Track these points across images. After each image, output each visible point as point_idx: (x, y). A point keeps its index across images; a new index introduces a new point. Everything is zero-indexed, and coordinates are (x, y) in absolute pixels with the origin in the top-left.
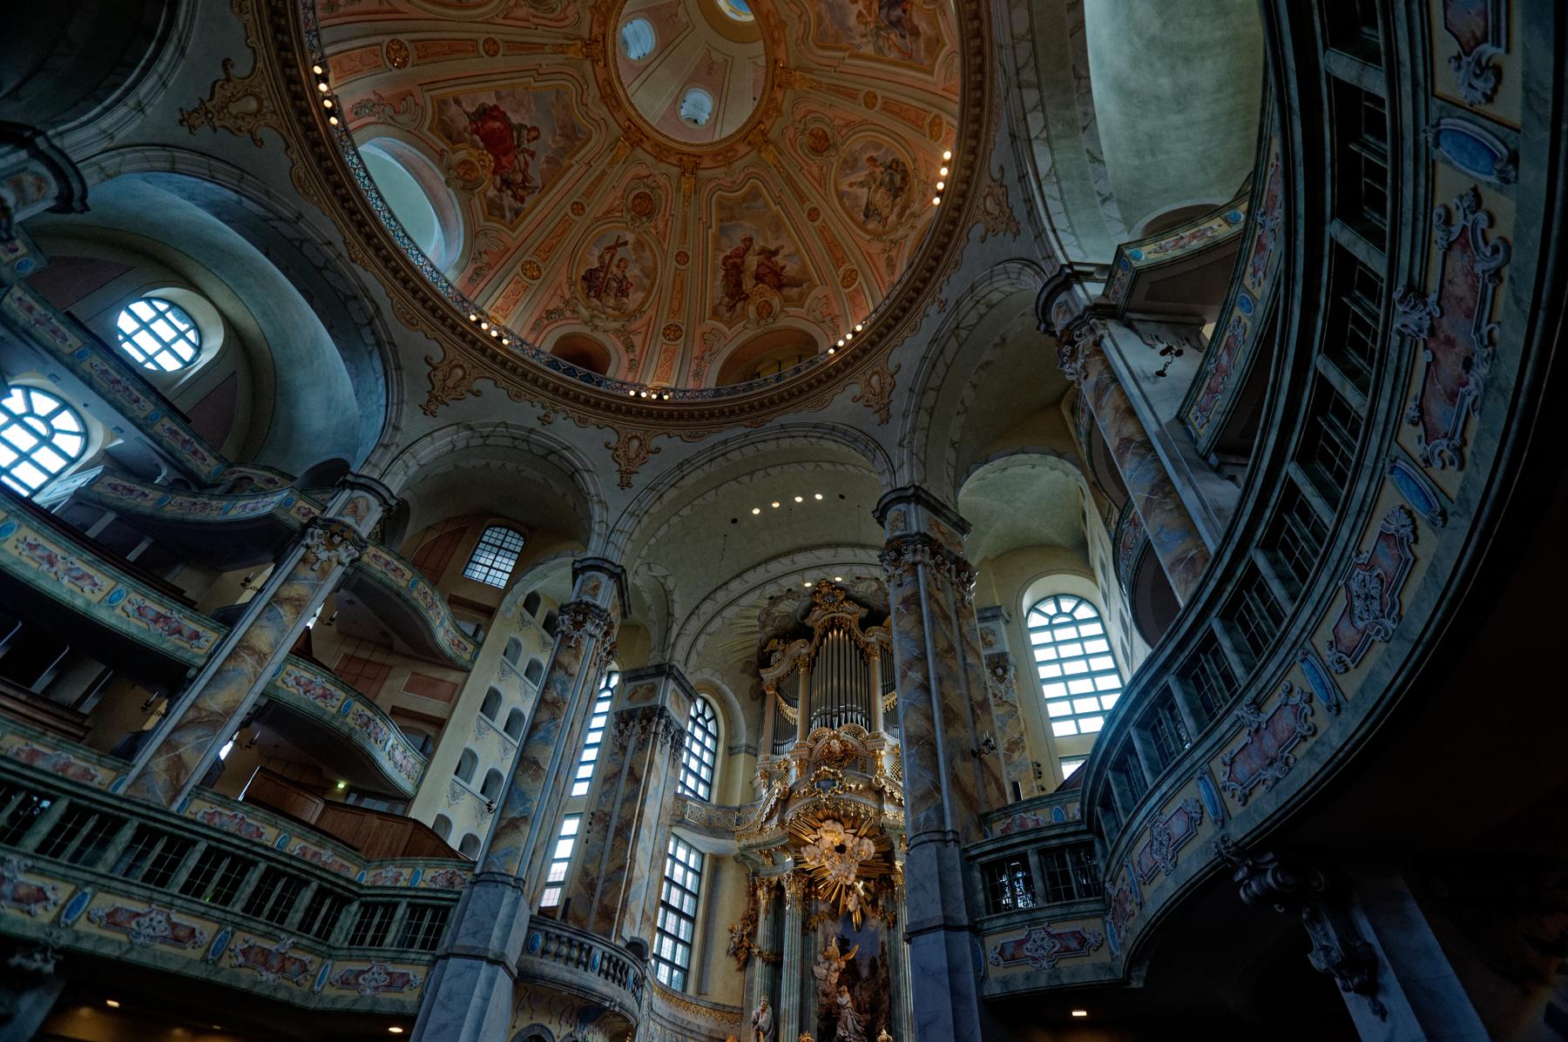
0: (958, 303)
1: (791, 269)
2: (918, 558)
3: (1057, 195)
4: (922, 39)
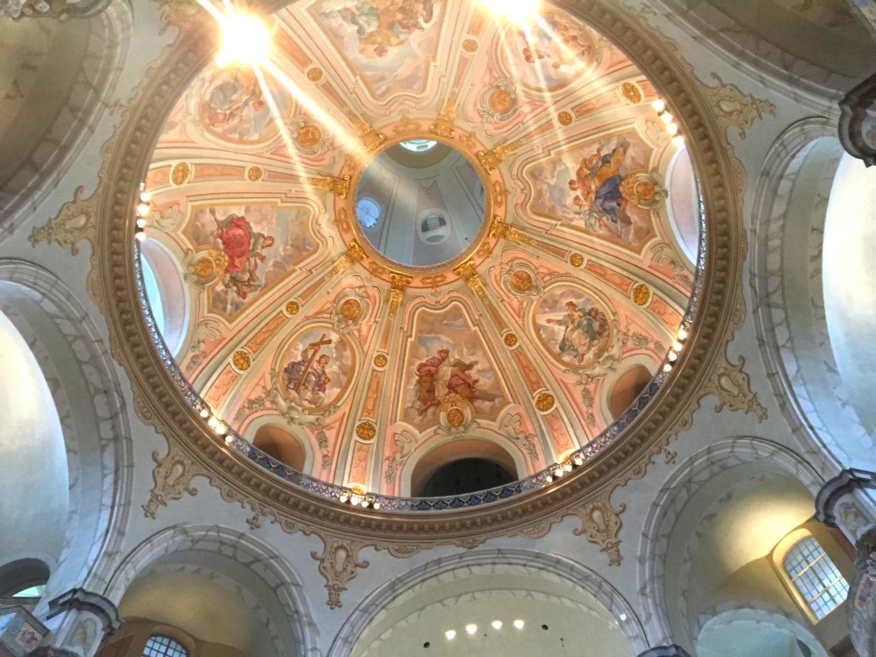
0: (692, 460)
1: (484, 383)
3: (806, 396)
4: (632, 226)
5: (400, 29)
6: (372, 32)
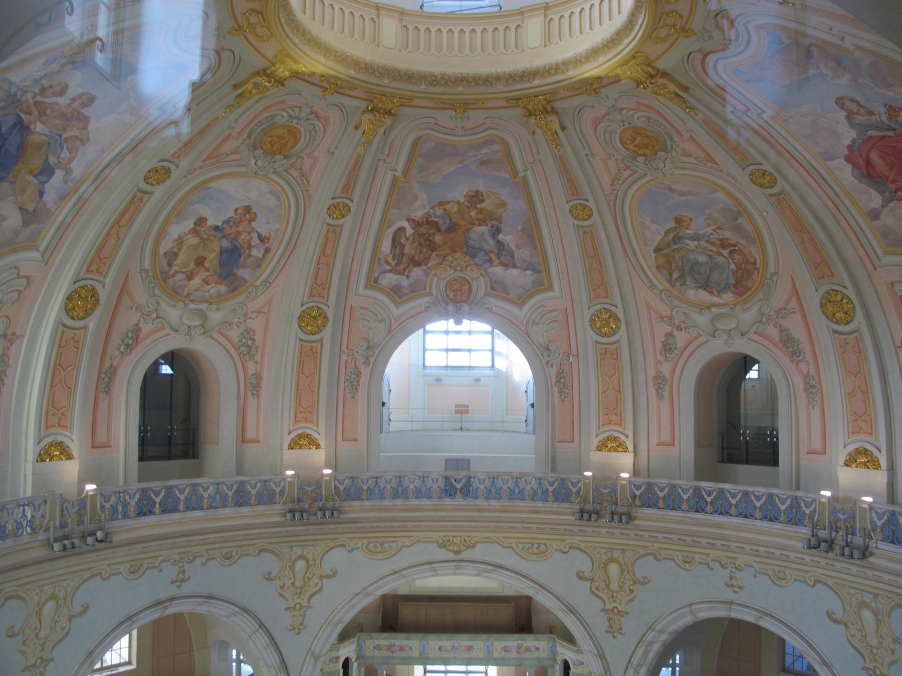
5: (440, 222)
6: (480, 225)
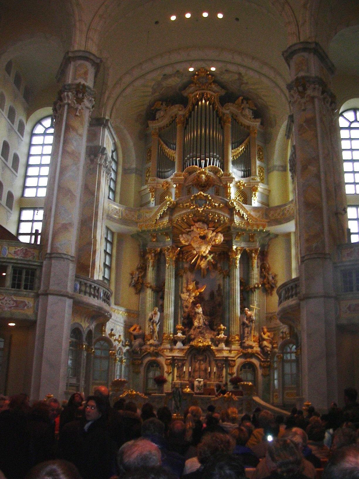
2: (316, 94)
